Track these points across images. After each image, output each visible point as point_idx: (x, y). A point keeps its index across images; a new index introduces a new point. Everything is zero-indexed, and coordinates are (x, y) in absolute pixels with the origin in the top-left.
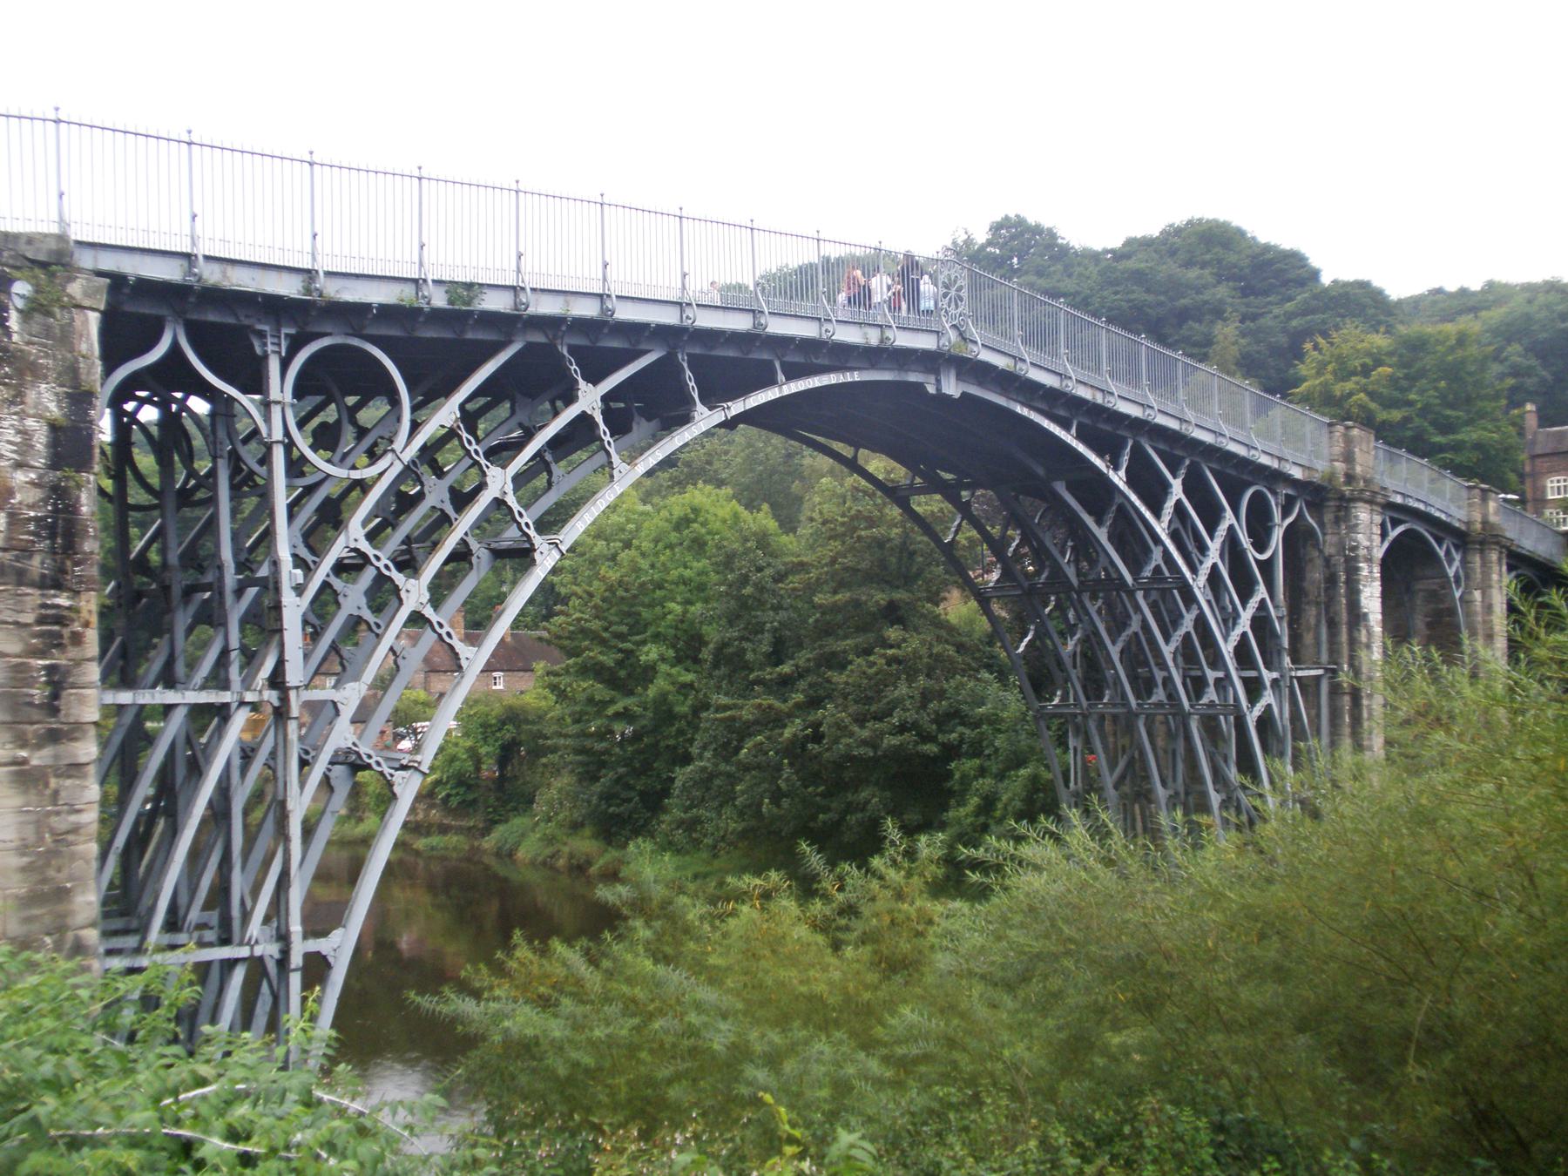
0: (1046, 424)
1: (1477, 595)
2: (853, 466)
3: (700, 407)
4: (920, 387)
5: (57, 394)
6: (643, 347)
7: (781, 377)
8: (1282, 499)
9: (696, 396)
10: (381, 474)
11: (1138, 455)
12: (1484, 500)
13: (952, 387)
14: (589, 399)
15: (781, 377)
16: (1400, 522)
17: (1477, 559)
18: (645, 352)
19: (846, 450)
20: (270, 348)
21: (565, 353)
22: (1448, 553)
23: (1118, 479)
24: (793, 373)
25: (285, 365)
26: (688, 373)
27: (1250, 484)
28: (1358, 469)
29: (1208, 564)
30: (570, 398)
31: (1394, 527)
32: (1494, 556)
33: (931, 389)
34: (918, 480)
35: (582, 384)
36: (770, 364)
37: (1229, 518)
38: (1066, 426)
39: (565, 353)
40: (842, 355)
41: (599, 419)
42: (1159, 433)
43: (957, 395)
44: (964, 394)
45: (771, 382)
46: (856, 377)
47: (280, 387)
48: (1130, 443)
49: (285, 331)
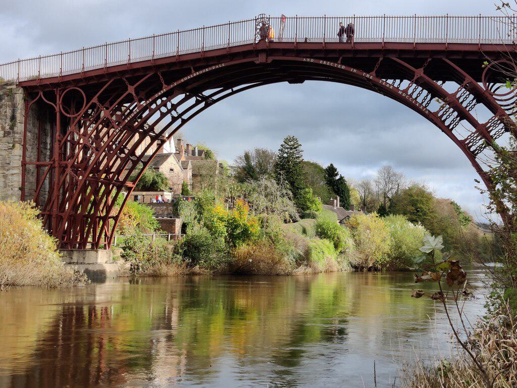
0: (321, 62)
4: (253, 63)
7: (193, 71)
9: (163, 83)
13: (261, 59)
14: (131, 90)
15: (193, 71)
18: (148, 74)
25: (60, 96)
26: (161, 77)
33: (257, 62)
36: (190, 68)
41: (134, 95)
43: (270, 61)
45: (190, 73)
47: (59, 101)
48: (381, 59)
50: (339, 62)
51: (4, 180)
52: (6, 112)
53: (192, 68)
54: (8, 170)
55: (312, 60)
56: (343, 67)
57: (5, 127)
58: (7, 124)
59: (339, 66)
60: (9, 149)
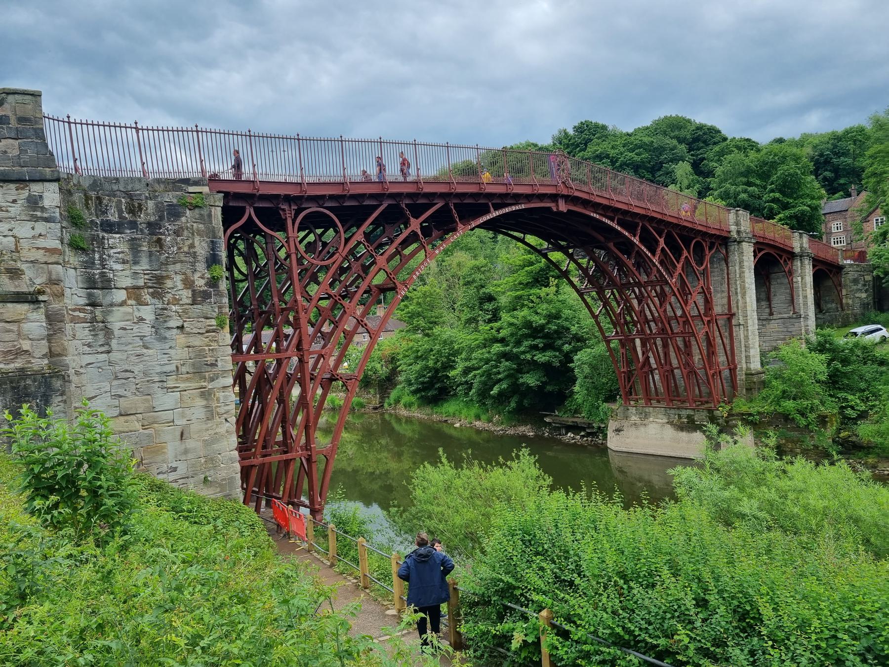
1: (799, 279)
2: (522, 241)
3: (460, 225)
4: (549, 208)
5: (207, 242)
6: (435, 202)
7: (492, 209)
8: (708, 243)
10: (334, 262)
11: (644, 228)
12: (801, 237)
13: (563, 207)
15: (492, 209)
16: (764, 249)
17: (799, 263)
18: (437, 204)
19: (521, 235)
20: (288, 215)
21: (404, 207)
22: (785, 261)
23: (636, 240)
24: (497, 207)
27: (694, 238)
28: (742, 228)
29: (677, 274)
30: (407, 224)
31: (760, 250)
32: (806, 262)
33: (555, 209)
34: (550, 246)
35: (412, 220)
37: (685, 253)
38: (612, 220)
39: (404, 207)
40: (517, 198)
41: (420, 233)
42: (652, 219)
44: (568, 210)
45: (488, 212)
46: (523, 206)
49: (293, 207)
50: (616, 222)
51: (204, 403)
52: (192, 246)
53: (490, 204)
54: (212, 380)
55: (598, 217)
56: (619, 229)
57: (193, 282)
58: (197, 275)
59: (616, 227)
60: (207, 332)
